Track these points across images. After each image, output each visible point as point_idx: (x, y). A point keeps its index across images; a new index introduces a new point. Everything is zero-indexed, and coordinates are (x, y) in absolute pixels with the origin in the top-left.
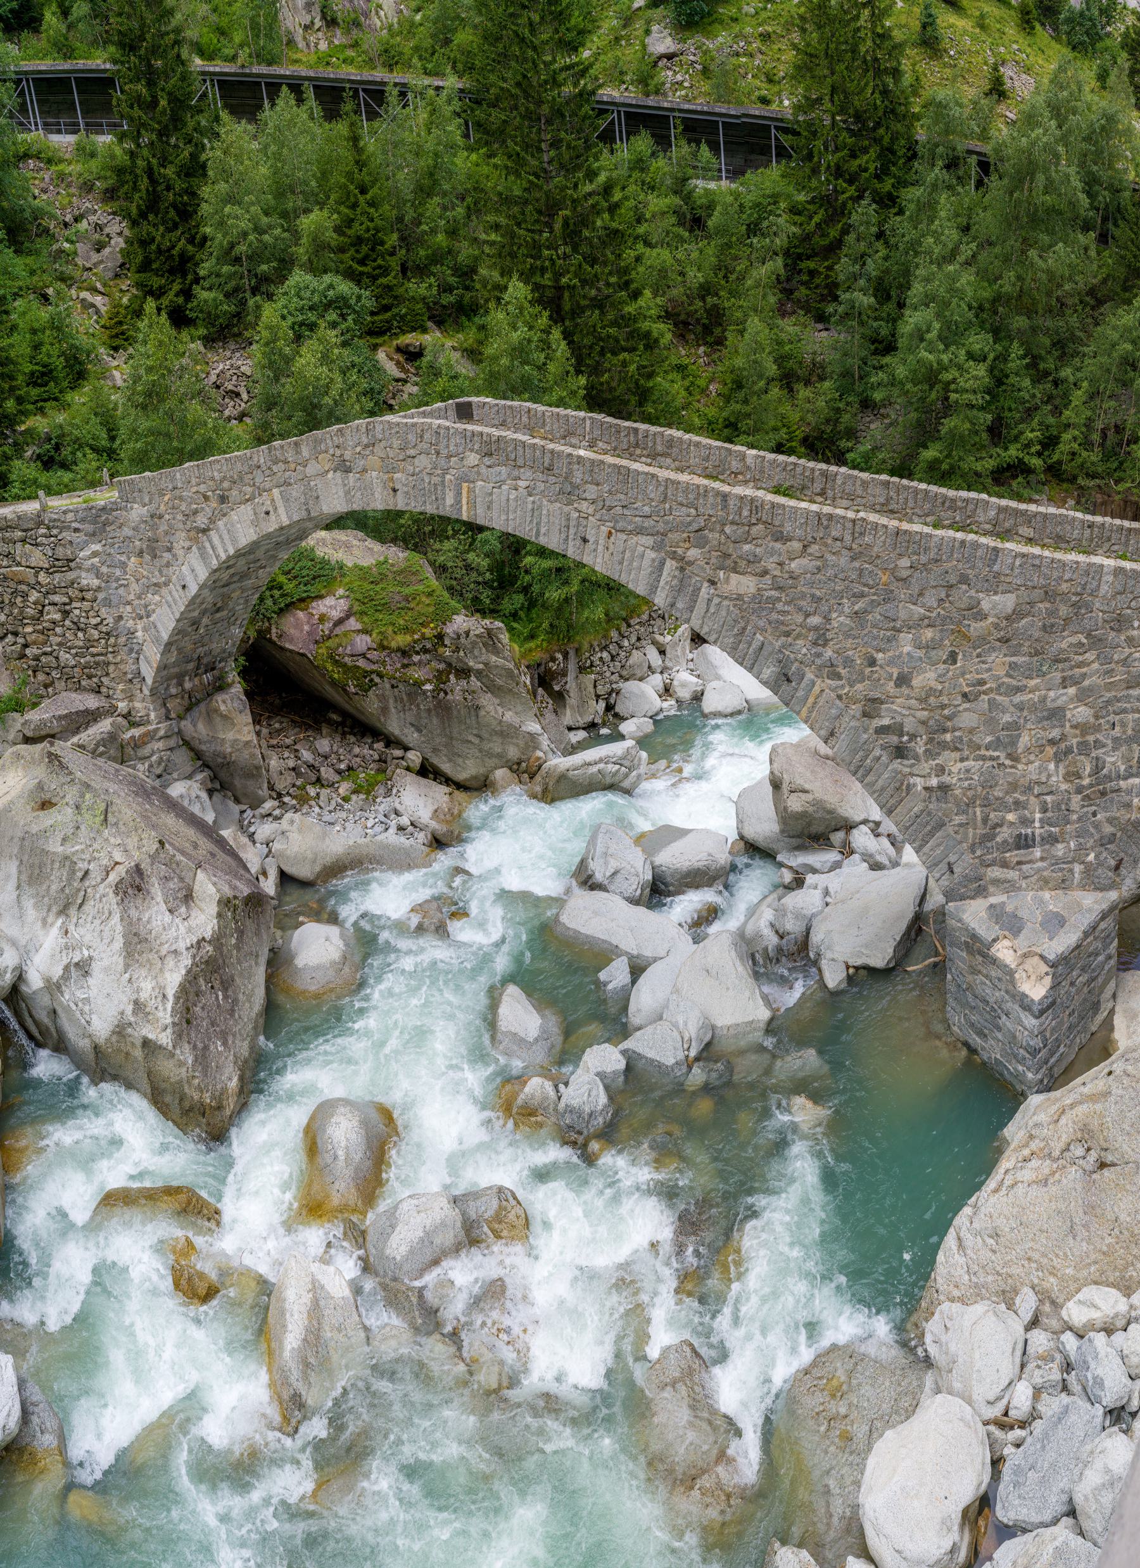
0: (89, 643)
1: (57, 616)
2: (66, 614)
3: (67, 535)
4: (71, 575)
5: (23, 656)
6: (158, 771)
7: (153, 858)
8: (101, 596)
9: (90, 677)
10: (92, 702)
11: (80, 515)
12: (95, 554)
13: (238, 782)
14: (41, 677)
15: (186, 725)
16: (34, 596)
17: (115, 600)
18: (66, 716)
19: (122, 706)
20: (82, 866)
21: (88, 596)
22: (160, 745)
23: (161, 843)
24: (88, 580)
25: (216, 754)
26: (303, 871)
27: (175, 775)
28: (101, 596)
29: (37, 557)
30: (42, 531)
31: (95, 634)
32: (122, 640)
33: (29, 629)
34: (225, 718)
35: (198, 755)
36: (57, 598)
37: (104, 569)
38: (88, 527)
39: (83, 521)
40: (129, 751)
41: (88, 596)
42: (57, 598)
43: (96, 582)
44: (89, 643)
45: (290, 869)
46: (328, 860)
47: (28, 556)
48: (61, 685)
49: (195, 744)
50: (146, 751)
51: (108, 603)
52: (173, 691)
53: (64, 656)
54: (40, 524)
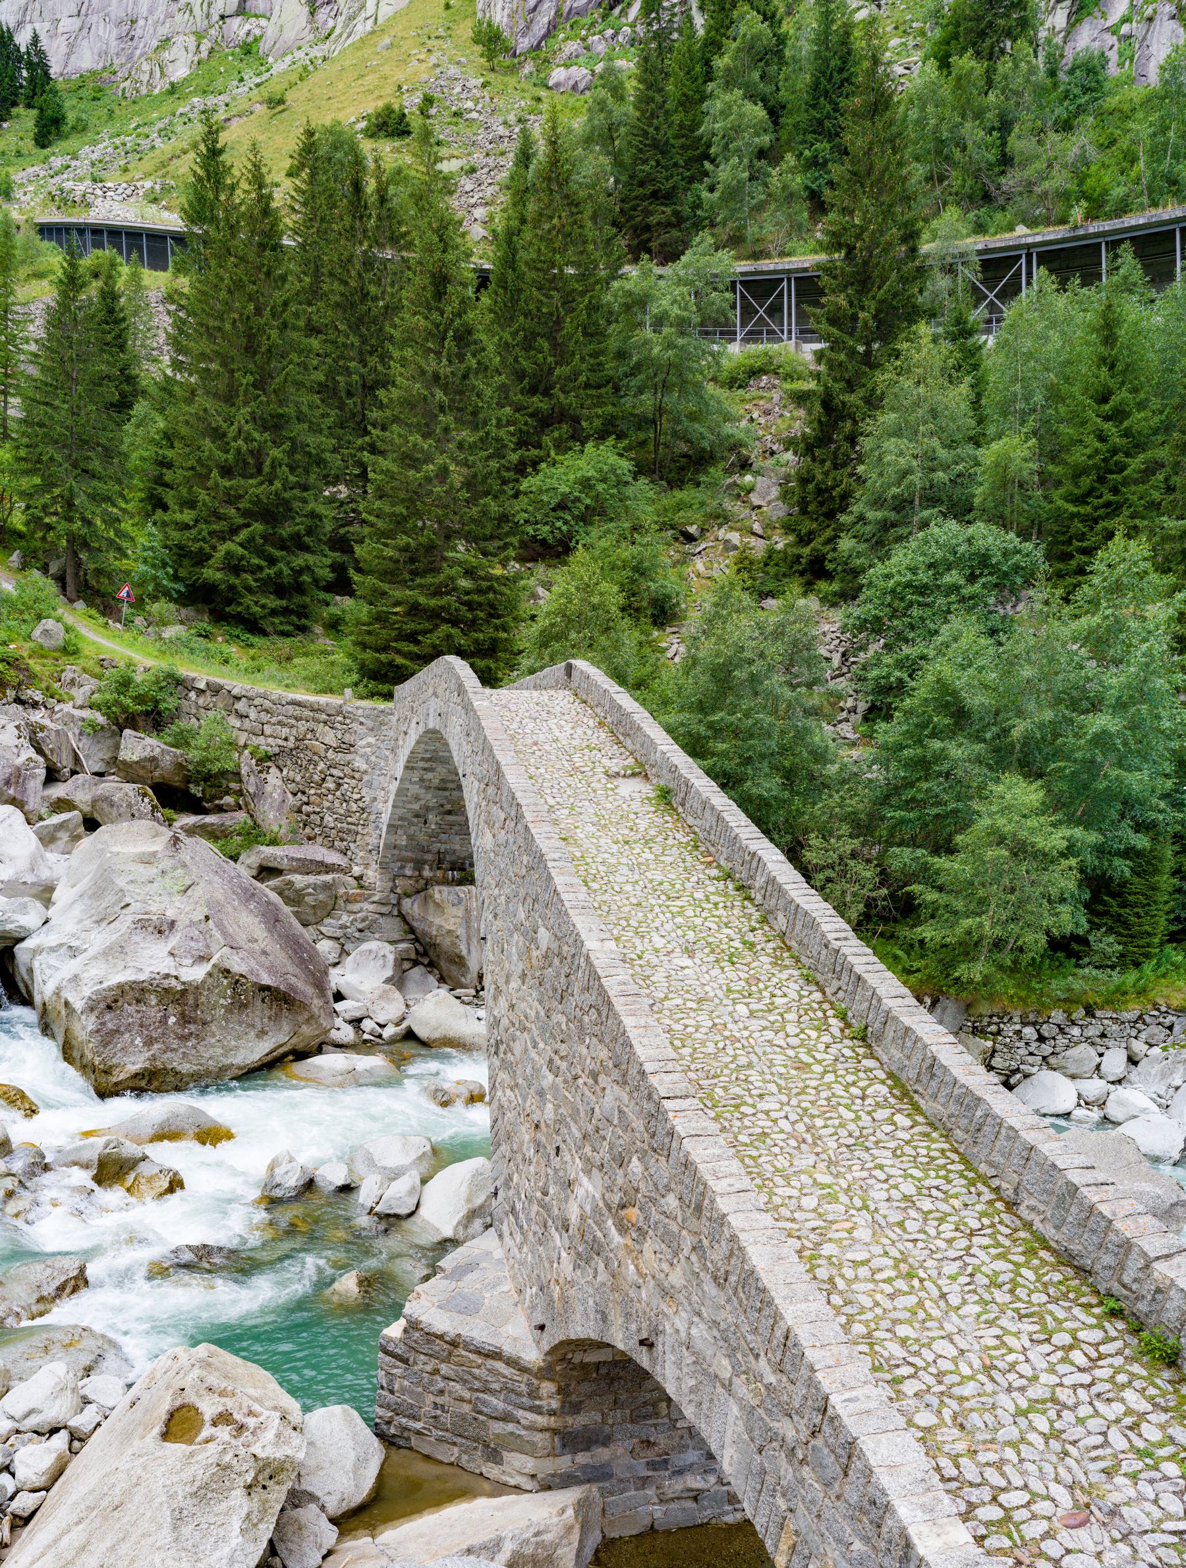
0: (349, 813)
1: (332, 786)
2: (339, 785)
3: (355, 726)
4: (349, 757)
5: (299, 811)
6: (360, 926)
7: (192, 924)
8: (366, 778)
9: (342, 840)
10: (333, 858)
11: (367, 712)
12: (369, 745)
13: (443, 964)
14: (308, 830)
15: (407, 903)
16: (321, 766)
17: (375, 784)
18: (299, 860)
19: (357, 870)
20: (128, 900)
21: (357, 775)
22: (371, 907)
23: (207, 918)
24: (360, 764)
25: (425, 934)
26: (422, 1033)
27: (377, 935)
28: (366, 778)
29: (330, 737)
30: (340, 718)
31: (354, 807)
32: (372, 817)
33: (312, 791)
34: (438, 905)
35: (412, 930)
36: (335, 772)
37: (373, 758)
38: (369, 723)
39: (367, 717)
40: (341, 902)
41: (357, 775)
42: (335, 772)
43: (364, 767)
44: (349, 813)
45: (416, 1029)
46: (451, 1034)
47: (324, 735)
48: (319, 840)
49: (409, 919)
50: (355, 907)
51: (370, 785)
52: (408, 872)
53: (329, 820)
54: (339, 713)
